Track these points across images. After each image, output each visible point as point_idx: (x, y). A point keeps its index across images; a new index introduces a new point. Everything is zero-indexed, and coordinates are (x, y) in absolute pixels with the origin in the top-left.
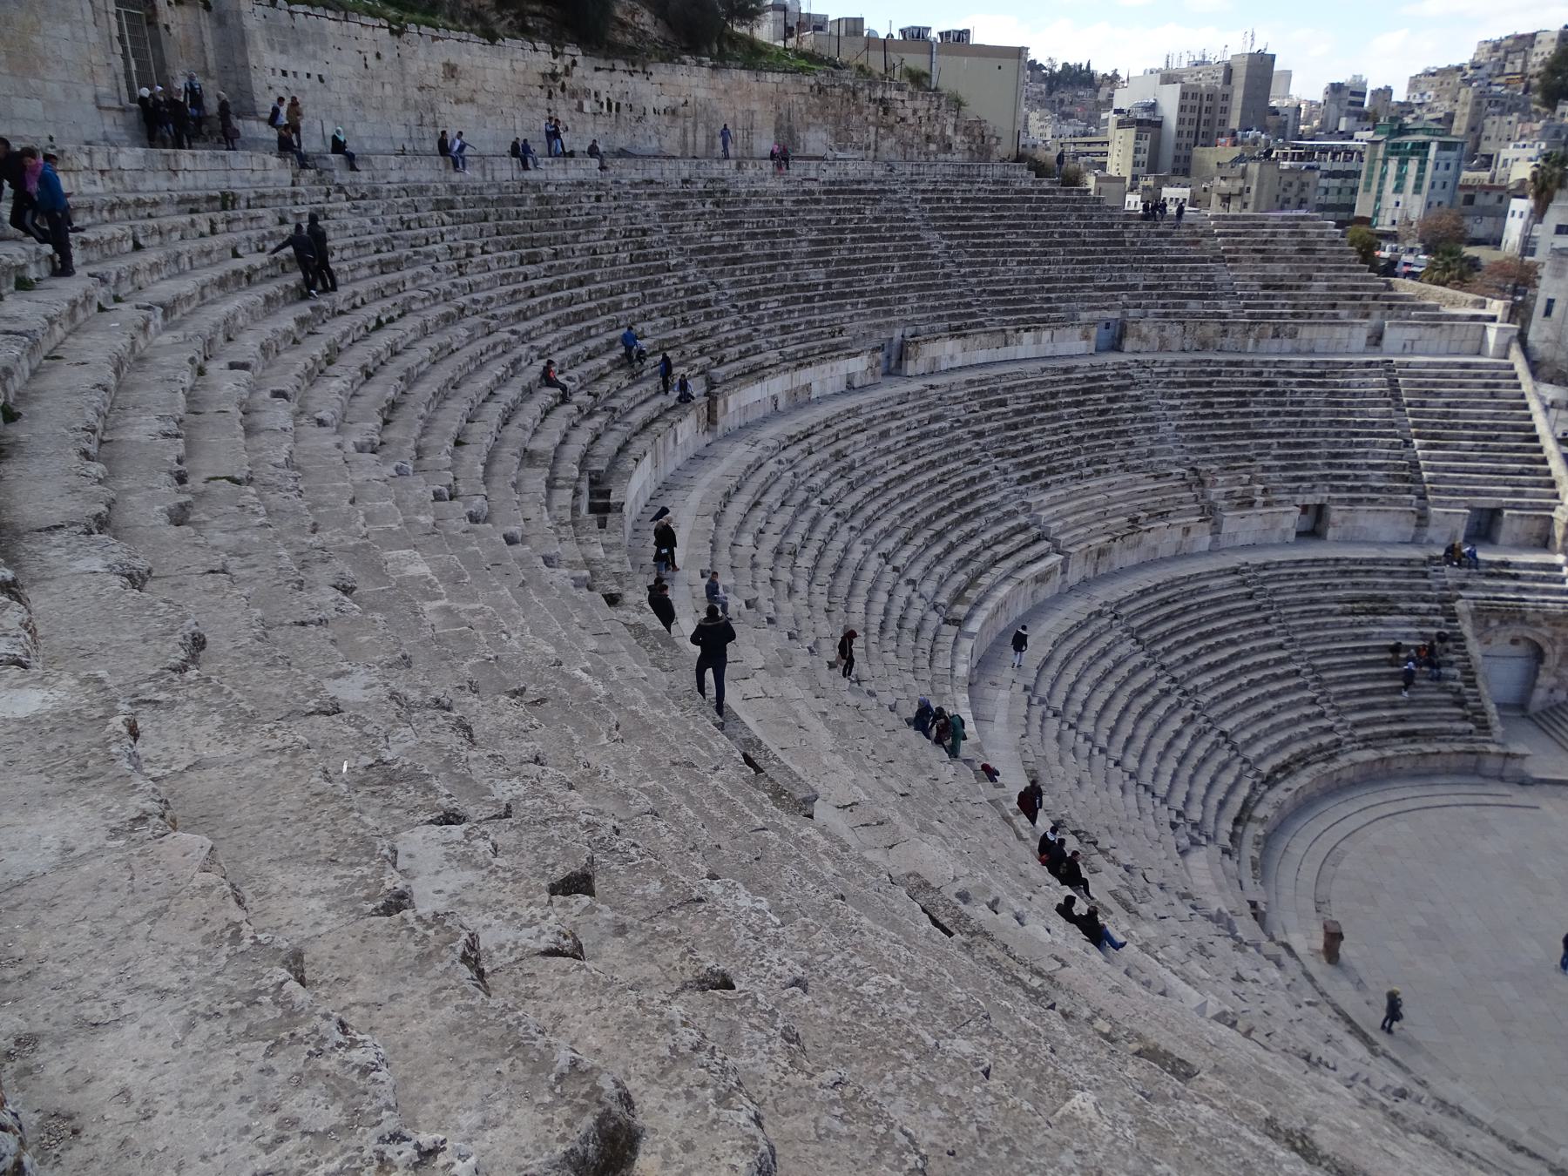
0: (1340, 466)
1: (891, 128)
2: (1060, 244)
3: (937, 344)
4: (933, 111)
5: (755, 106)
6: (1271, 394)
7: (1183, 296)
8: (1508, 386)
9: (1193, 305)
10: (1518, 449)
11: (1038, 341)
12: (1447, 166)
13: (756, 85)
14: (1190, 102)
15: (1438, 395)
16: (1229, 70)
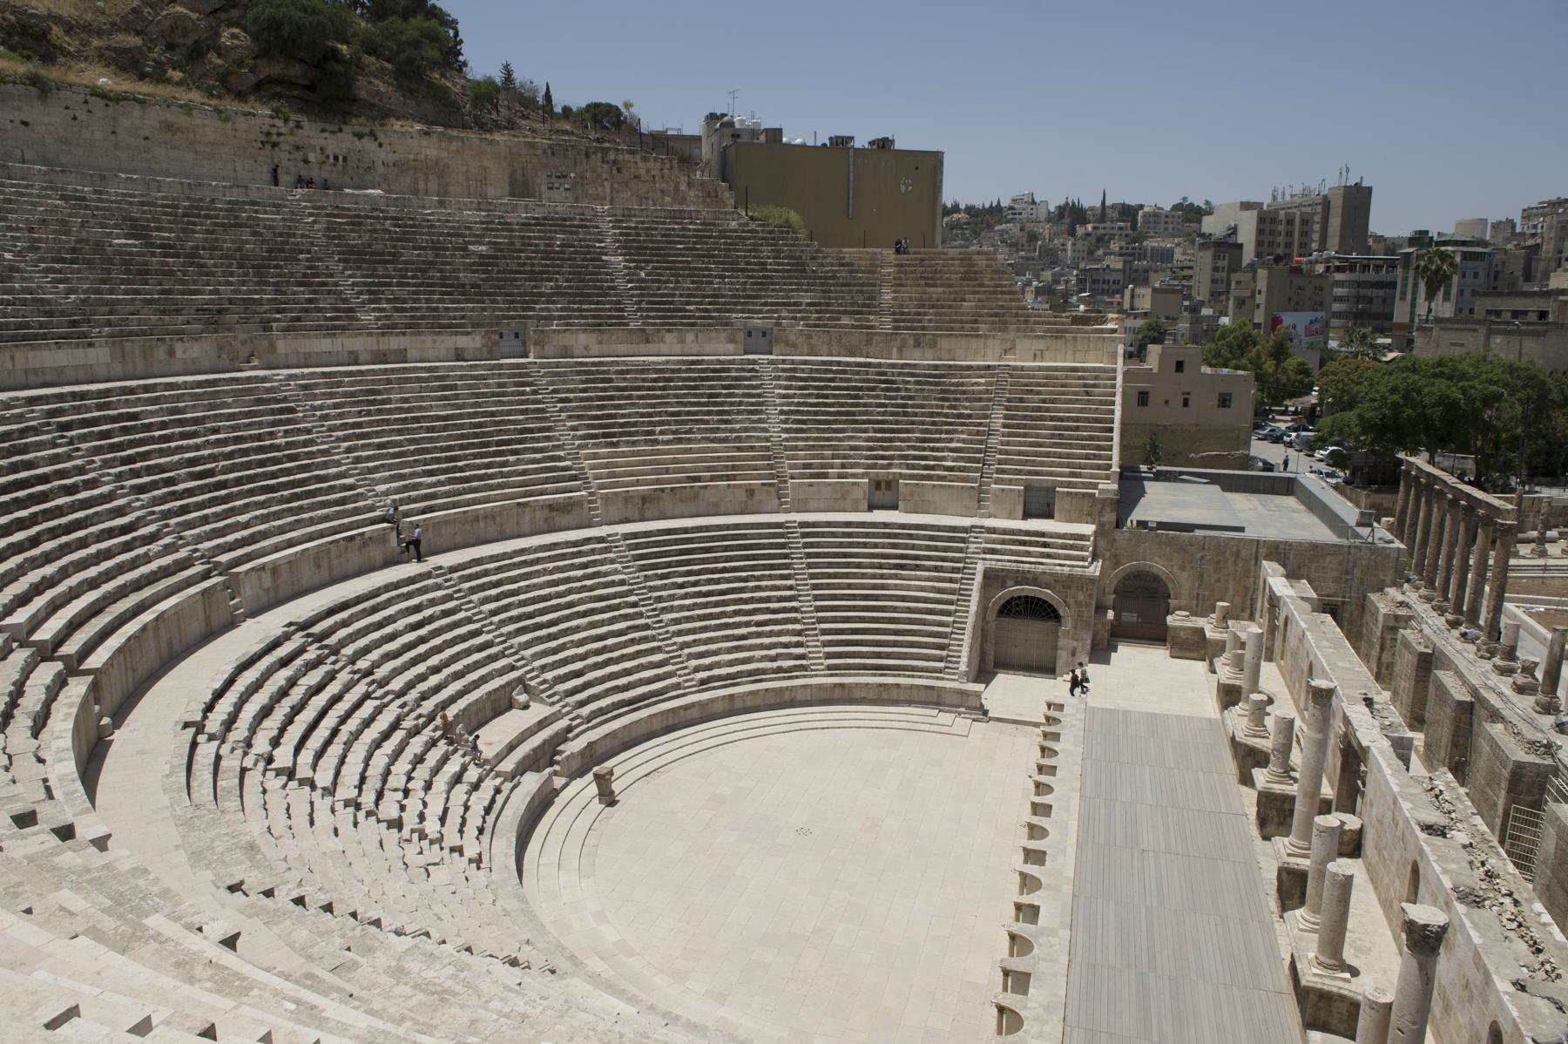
0: (924, 449)
1: (627, 184)
2: (742, 270)
3: (567, 335)
4: (666, 172)
5: (486, 163)
6: (887, 390)
7: (839, 312)
8: (1105, 386)
9: (845, 321)
10: (1091, 438)
11: (682, 341)
12: (1476, 275)
13: (488, 148)
14: (1267, 226)
15: (1039, 393)
16: (1326, 203)
